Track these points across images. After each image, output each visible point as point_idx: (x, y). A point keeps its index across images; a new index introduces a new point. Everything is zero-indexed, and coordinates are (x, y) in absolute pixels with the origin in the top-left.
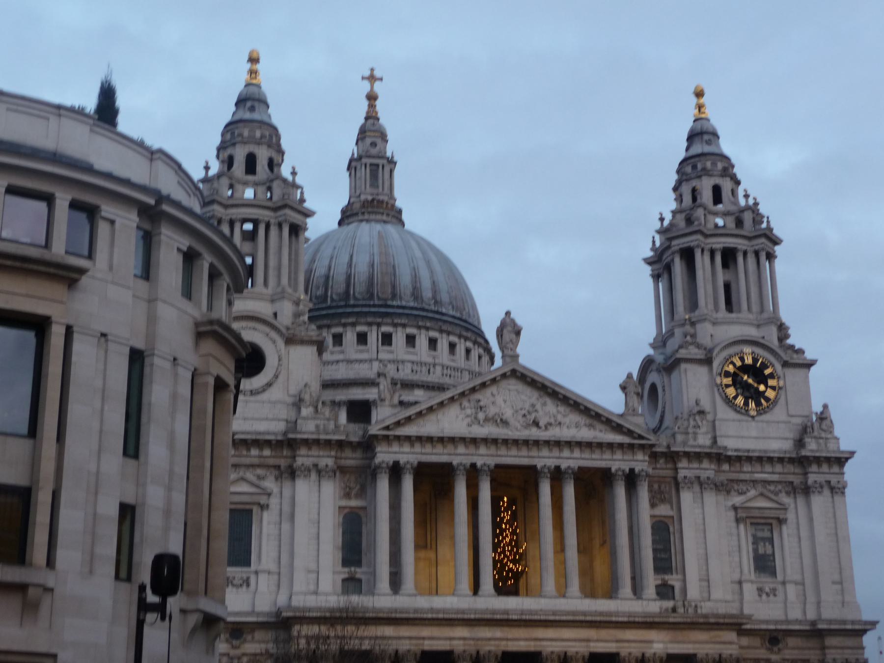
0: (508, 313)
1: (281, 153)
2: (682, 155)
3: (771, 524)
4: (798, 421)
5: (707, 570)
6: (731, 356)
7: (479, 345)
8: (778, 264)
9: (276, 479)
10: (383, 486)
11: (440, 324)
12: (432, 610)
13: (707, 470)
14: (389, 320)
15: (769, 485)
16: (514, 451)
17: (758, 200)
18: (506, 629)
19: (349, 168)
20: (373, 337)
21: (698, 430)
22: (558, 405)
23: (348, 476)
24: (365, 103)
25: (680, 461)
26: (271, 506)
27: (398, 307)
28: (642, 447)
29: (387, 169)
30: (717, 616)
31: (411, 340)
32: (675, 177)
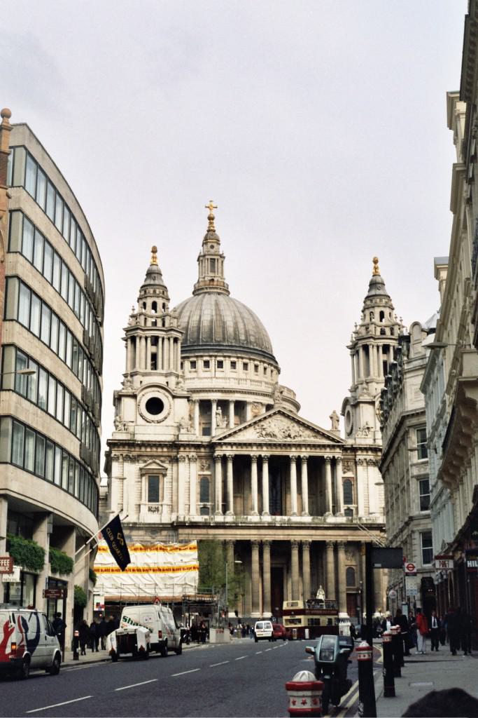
1: (168, 300)
2: (366, 294)
7: (271, 365)
9: (170, 462)
10: (219, 467)
11: (250, 355)
13: (370, 456)
14: (221, 354)
16: (279, 449)
19: (198, 260)
20: (213, 363)
23: (203, 460)
27: (226, 346)
28: (339, 446)
29: (220, 261)
31: (233, 364)
32: (363, 305)
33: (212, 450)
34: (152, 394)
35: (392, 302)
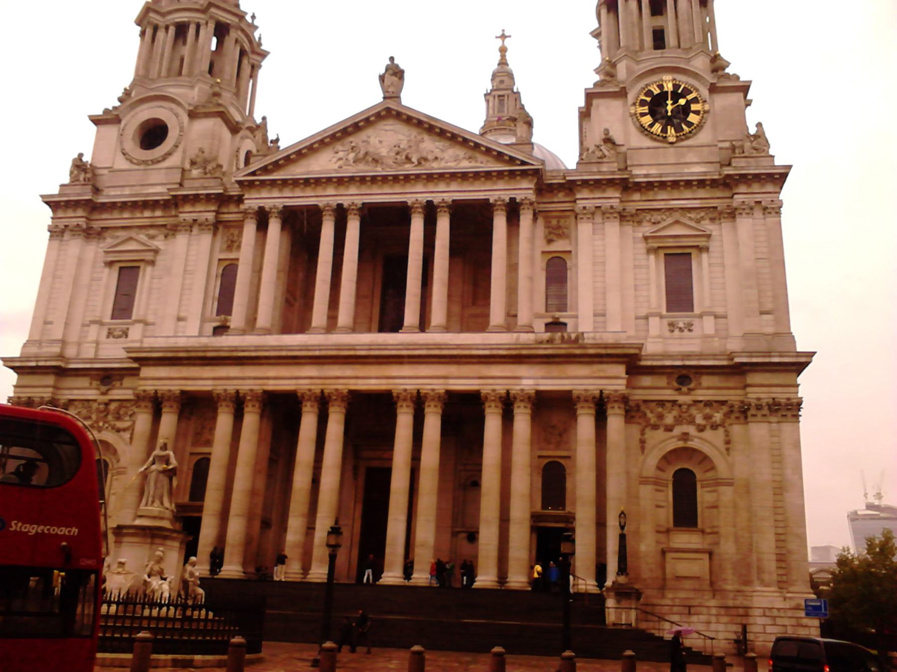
0: (392, 59)
3: (690, 254)
4: (727, 145)
5: (605, 305)
6: (647, 85)
9: (166, 237)
10: (250, 230)
12: (274, 348)
13: (612, 198)
15: (690, 213)
18: (358, 367)
21: (605, 160)
23: (232, 230)
24: (499, 54)
25: (580, 191)
26: (157, 263)
34: (146, 113)
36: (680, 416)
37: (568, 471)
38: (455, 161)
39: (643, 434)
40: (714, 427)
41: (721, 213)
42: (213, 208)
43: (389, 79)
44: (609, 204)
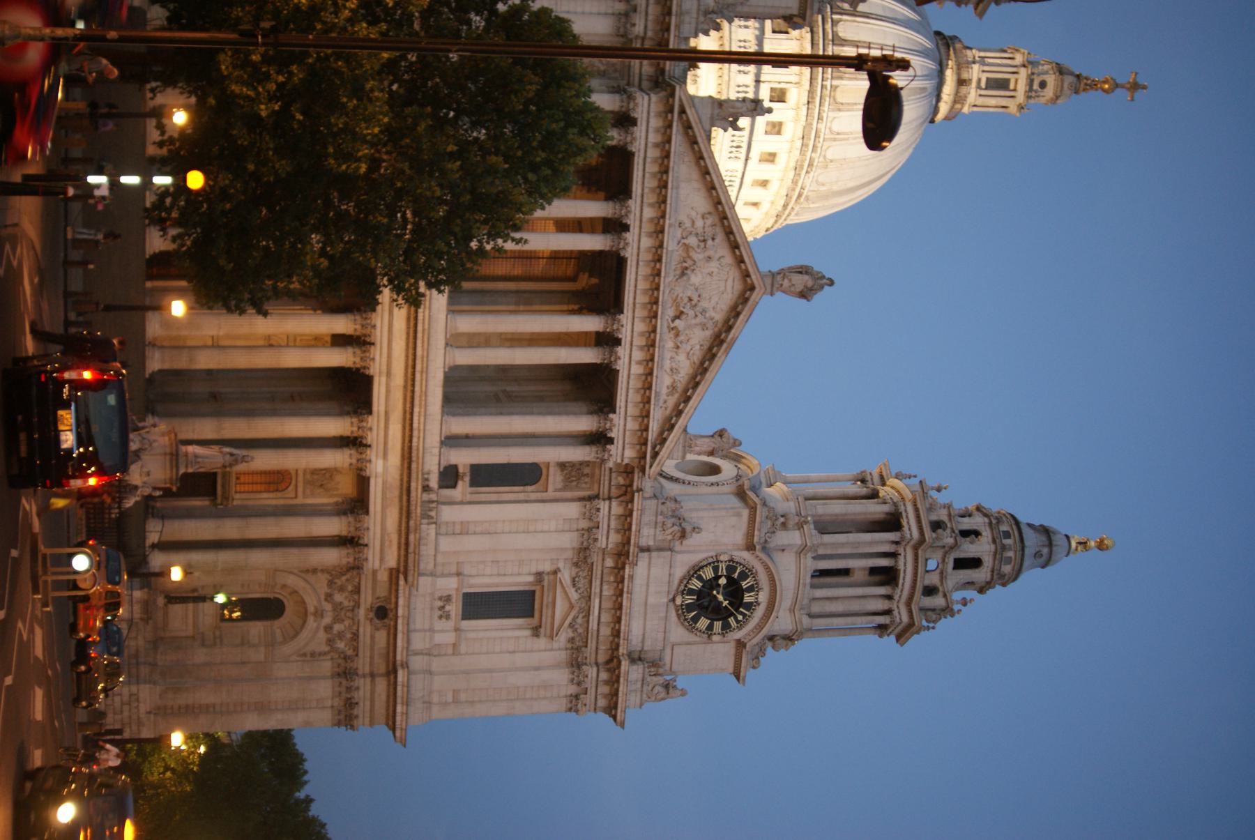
0: (831, 283)
2: (1023, 519)
3: (532, 616)
4: (667, 659)
6: (755, 575)
8: (873, 638)
13: (608, 539)
16: (642, 285)
17: (957, 616)
21: (659, 529)
22: (701, 345)
25: (620, 505)
28: (644, 457)
30: (418, 545)
33: (645, 84)
35: (998, 587)
36: (342, 609)
37: (279, 494)
38: (671, 370)
39: (322, 571)
40: (330, 642)
41: (578, 649)
42: (650, 34)
43: (800, 281)
44: (600, 538)
